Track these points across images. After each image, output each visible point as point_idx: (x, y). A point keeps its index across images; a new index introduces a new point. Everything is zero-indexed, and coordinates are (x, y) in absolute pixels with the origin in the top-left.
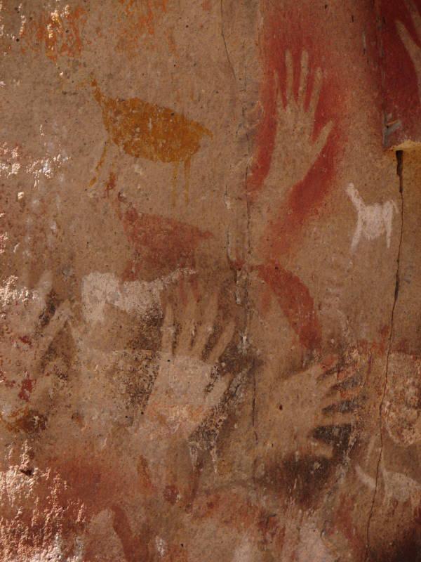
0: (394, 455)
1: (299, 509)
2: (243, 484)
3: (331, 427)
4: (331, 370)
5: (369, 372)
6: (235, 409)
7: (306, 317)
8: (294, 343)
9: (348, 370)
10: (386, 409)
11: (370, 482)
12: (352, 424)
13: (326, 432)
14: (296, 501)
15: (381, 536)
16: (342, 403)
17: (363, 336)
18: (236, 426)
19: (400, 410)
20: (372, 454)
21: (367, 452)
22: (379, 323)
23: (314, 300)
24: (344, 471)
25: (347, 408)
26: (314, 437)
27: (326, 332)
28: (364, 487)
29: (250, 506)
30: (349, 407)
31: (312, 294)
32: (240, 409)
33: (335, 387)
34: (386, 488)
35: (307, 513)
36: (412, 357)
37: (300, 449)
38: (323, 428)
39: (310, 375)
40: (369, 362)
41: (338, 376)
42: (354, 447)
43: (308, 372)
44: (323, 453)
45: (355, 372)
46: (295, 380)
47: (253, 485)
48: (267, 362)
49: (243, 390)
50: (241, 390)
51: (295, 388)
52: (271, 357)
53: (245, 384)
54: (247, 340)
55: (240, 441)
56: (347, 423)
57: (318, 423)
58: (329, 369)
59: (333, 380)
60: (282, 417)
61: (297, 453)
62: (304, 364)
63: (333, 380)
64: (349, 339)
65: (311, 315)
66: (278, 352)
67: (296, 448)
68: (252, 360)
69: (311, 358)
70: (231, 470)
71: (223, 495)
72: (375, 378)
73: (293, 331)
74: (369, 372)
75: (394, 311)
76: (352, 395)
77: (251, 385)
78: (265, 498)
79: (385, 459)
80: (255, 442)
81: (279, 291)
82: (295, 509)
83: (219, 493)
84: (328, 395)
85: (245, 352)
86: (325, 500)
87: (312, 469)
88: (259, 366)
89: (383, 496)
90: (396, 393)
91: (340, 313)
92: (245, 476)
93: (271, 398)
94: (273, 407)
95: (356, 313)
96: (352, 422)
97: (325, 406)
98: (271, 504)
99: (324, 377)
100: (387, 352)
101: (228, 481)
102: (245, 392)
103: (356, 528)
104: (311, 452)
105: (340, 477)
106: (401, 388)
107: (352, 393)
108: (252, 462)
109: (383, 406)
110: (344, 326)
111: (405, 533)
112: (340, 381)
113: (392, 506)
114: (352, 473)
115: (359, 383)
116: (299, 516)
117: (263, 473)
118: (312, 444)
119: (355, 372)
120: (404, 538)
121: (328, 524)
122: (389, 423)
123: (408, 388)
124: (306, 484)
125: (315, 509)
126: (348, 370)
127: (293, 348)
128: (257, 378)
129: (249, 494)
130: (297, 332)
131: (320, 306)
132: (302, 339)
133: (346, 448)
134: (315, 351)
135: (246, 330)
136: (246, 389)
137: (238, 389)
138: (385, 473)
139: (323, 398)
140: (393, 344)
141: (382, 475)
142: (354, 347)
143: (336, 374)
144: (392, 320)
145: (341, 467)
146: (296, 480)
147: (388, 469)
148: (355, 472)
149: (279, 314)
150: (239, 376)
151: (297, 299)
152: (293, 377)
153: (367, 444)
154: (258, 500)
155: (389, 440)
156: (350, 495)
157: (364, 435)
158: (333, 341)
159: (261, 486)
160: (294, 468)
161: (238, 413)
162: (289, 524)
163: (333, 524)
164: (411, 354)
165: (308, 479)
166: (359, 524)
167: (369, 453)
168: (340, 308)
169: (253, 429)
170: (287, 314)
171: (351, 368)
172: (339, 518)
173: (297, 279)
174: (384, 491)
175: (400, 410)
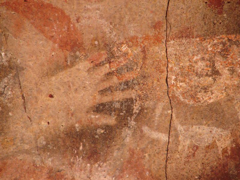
0: (188, 114)
1: (86, 164)
2: (27, 152)
3: (111, 102)
4: (101, 63)
5: (145, 58)
6: (7, 103)
7: (64, 30)
8: (53, 50)
9: (119, 60)
10: (173, 82)
11: (163, 137)
12: (134, 98)
13: (107, 106)
14: (82, 159)
15: (184, 173)
16: (120, 84)
17: (132, 33)
18: (10, 114)
19: (190, 80)
20: (160, 116)
21: (155, 115)
22: (150, 21)
23: (71, 17)
24: (130, 132)
25: (126, 87)
26: (94, 111)
27: (87, 38)
28: (153, 142)
29: (36, 167)
30: (128, 85)
31: (67, 13)
32: (10, 103)
33: (110, 74)
34: (181, 138)
35: (97, 165)
36: (198, 39)
37: (80, 122)
38: (103, 105)
39: (79, 70)
40: (144, 51)
41: (110, 66)
42: (139, 114)
43: (77, 67)
44: (105, 122)
45: (127, 61)
46: (63, 76)
47: (37, 152)
48: (27, 68)
49: (10, 89)
50: (8, 89)
51: (66, 80)
52: (31, 64)
53: (12, 85)
54: (6, 55)
55: (17, 124)
56: (128, 97)
57: (97, 101)
58: (97, 63)
59: (106, 69)
60: (56, 102)
61: (77, 125)
62: (69, 63)
63: (106, 69)
64: (116, 38)
65: (68, 28)
66: (37, 59)
67: (75, 122)
68: (15, 68)
69: (77, 57)
70: (14, 144)
71: (9, 162)
72: (154, 62)
73: (51, 43)
74: (145, 58)
75: (169, 9)
76: (129, 77)
77: (17, 85)
78: (50, 159)
79: (177, 118)
80: (31, 123)
81: (31, 16)
82: (83, 164)
83: (5, 160)
84: (103, 81)
85: (6, 64)
86: (115, 154)
87: (96, 134)
88: (20, 71)
89: (177, 145)
90: (182, 68)
91: (103, 21)
92: (27, 147)
93: (40, 92)
94: (43, 97)
95: (121, 19)
96: (133, 96)
97: (101, 89)
98: (57, 163)
99: (94, 69)
100: (164, 41)
101: (13, 152)
102: (11, 91)
103: (150, 171)
104: (92, 123)
105: (126, 136)
106: (188, 64)
107: (128, 76)
108: (33, 137)
109: (168, 80)
110: (107, 30)
111: (212, 168)
112: (113, 69)
113: (191, 150)
114: (139, 135)
115: (135, 68)
116: (88, 169)
117: (44, 143)
118: (93, 116)
119: (127, 61)
120: (212, 171)
121: (117, 171)
122: (178, 93)
123: (196, 62)
124: (93, 145)
125: (105, 161)
126: (119, 60)
127: (53, 54)
128: (21, 79)
129: (34, 158)
130: (55, 42)
131: (78, 20)
132: (61, 47)
133: (132, 115)
134: (78, 53)
135: (3, 48)
136: (12, 88)
137: (6, 89)
138: (180, 128)
139: (98, 83)
140: (171, 34)
141: (176, 130)
142: (123, 43)
143: (108, 65)
144: (166, 16)
145: (126, 130)
146: (81, 144)
147: (182, 125)
148: (142, 131)
149: (34, 33)
150: (6, 80)
151: (51, 19)
152: (61, 73)
153: (153, 110)
154: (42, 162)
155: (179, 103)
156: (138, 148)
157: (149, 104)
158: (96, 43)
159: (44, 151)
160: (77, 136)
161: (9, 105)
162: (78, 175)
163: (122, 171)
164: (196, 38)
165: (95, 141)
166: (154, 167)
167: (157, 116)
168: (101, 17)
169: (25, 115)
170: (43, 32)
171: (122, 59)
172: (129, 166)
173: (50, 6)
174: (179, 141)
175: (190, 80)
